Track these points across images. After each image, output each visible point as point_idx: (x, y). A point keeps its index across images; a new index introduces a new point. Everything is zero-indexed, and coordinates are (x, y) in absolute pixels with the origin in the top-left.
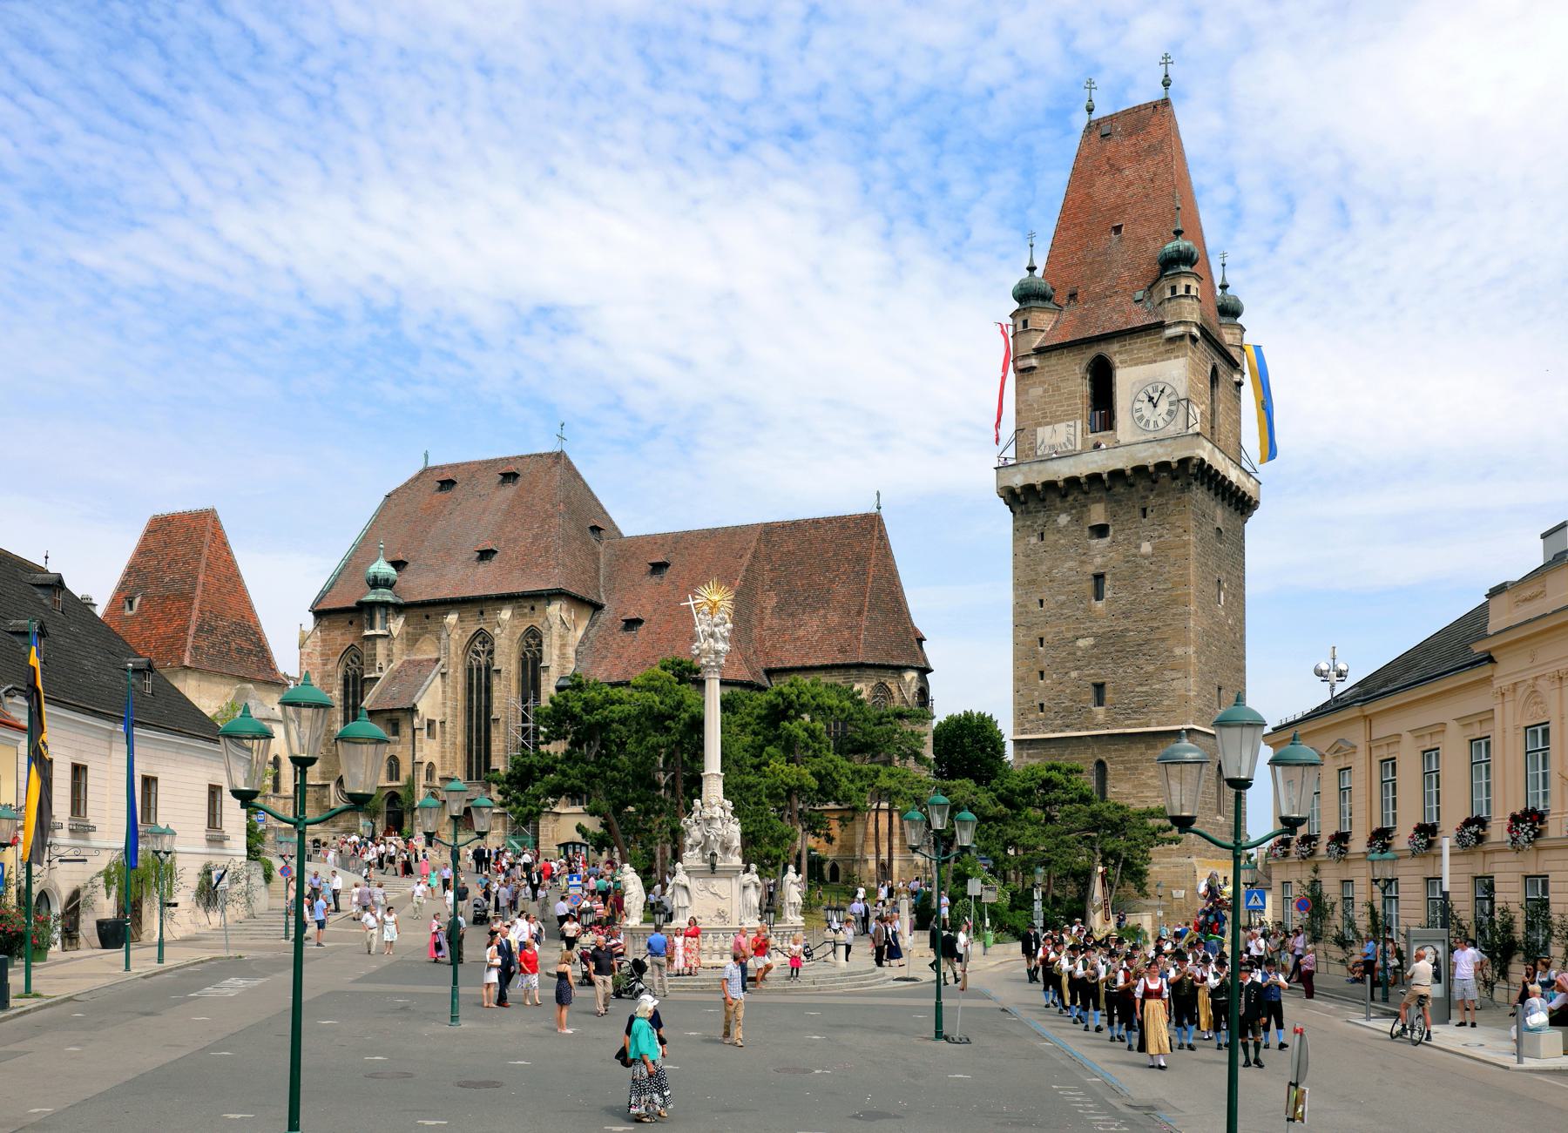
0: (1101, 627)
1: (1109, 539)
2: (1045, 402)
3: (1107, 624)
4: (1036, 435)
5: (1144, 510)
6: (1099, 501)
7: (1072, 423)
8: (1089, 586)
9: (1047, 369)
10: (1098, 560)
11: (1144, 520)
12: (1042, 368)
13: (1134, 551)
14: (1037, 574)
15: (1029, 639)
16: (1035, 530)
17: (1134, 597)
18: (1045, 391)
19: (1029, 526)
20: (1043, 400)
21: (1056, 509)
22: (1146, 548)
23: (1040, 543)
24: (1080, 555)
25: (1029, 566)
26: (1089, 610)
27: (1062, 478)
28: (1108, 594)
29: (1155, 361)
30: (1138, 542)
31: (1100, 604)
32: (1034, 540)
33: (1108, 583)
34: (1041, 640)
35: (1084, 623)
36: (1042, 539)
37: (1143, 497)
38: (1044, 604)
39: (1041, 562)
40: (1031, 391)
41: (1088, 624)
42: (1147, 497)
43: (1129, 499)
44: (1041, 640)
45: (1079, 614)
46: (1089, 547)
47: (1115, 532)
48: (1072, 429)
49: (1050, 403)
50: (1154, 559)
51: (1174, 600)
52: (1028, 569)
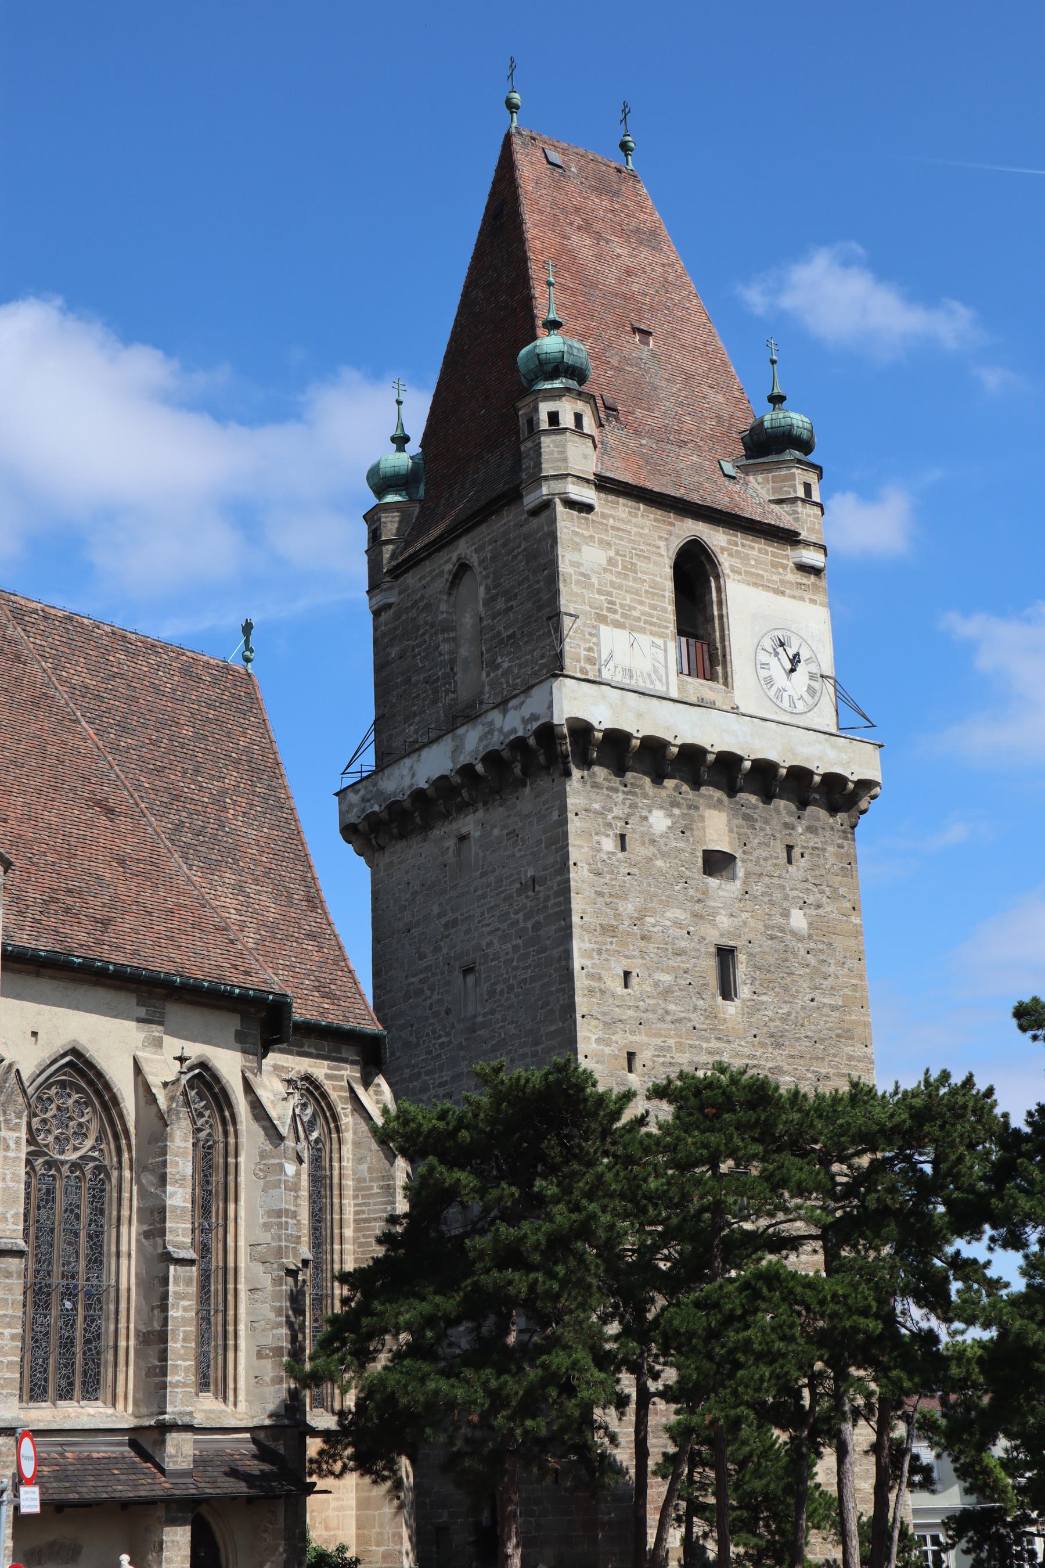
0: (737, 1055)
1: (738, 883)
2: (612, 584)
3: (747, 1051)
4: (597, 636)
5: (790, 848)
6: (718, 805)
7: (660, 642)
8: (710, 965)
9: (611, 521)
10: (724, 921)
11: (790, 868)
12: (604, 516)
13: (779, 920)
14: (617, 916)
15: (607, 1050)
16: (609, 825)
17: (785, 1009)
18: (610, 560)
19: (597, 813)
20: (609, 577)
21: (645, 796)
22: (798, 920)
23: (620, 855)
24: (691, 899)
25: (600, 894)
26: (712, 1015)
27: (679, 742)
28: (744, 991)
29: (783, 593)
30: (786, 904)
31: (731, 1009)
32: (609, 844)
33: (742, 969)
34: (631, 1056)
35: (707, 1040)
36: (623, 848)
37: (787, 826)
38: (634, 981)
39: (623, 895)
40: (585, 548)
41: (714, 1044)
42: (793, 828)
43: (766, 822)
44: (631, 1056)
45: (697, 1019)
46: (706, 892)
47: (748, 875)
48: (661, 653)
49: (620, 587)
50: (812, 945)
51: (849, 1030)
52: (599, 899)
